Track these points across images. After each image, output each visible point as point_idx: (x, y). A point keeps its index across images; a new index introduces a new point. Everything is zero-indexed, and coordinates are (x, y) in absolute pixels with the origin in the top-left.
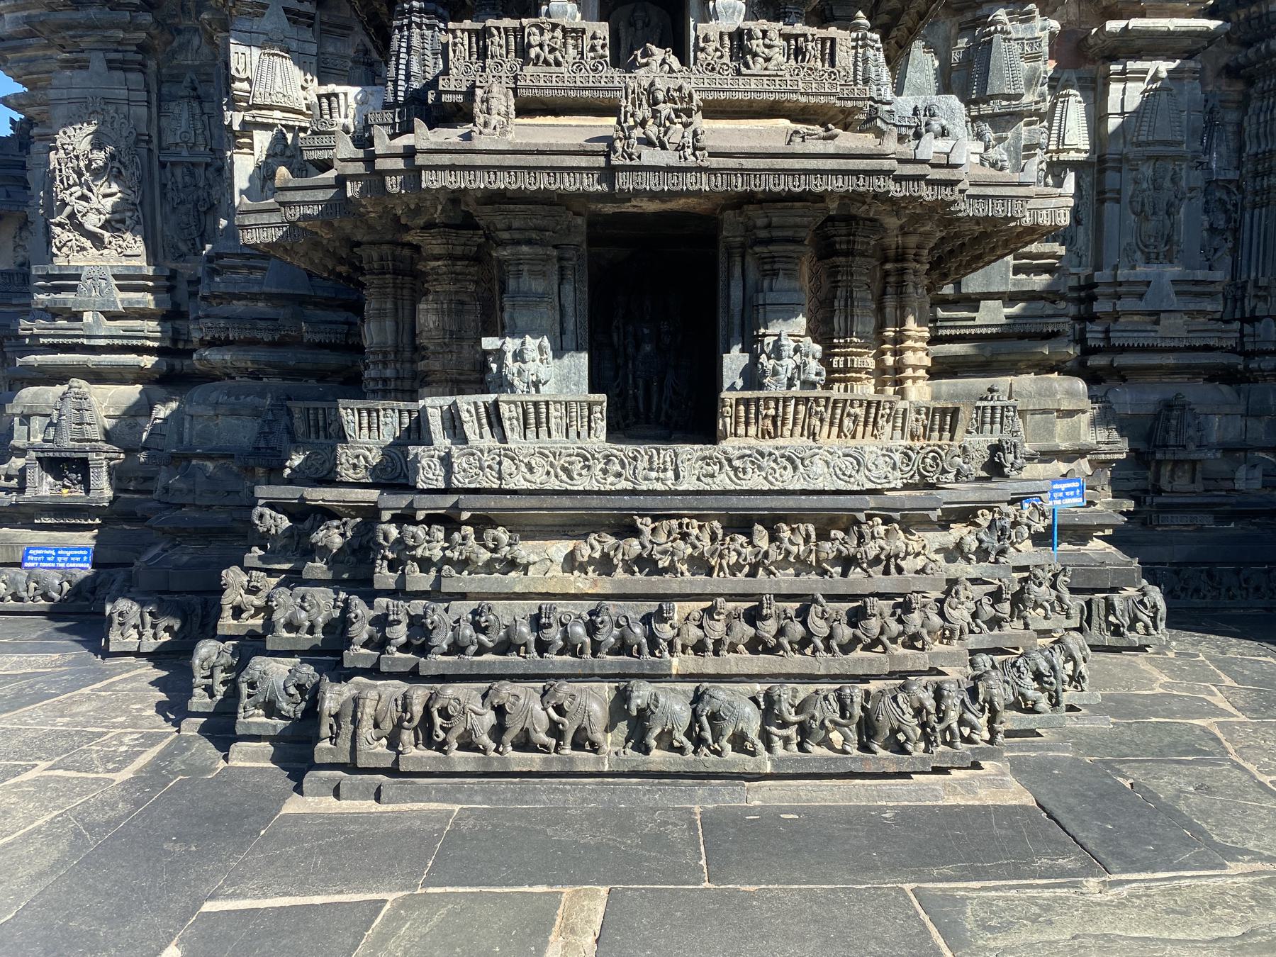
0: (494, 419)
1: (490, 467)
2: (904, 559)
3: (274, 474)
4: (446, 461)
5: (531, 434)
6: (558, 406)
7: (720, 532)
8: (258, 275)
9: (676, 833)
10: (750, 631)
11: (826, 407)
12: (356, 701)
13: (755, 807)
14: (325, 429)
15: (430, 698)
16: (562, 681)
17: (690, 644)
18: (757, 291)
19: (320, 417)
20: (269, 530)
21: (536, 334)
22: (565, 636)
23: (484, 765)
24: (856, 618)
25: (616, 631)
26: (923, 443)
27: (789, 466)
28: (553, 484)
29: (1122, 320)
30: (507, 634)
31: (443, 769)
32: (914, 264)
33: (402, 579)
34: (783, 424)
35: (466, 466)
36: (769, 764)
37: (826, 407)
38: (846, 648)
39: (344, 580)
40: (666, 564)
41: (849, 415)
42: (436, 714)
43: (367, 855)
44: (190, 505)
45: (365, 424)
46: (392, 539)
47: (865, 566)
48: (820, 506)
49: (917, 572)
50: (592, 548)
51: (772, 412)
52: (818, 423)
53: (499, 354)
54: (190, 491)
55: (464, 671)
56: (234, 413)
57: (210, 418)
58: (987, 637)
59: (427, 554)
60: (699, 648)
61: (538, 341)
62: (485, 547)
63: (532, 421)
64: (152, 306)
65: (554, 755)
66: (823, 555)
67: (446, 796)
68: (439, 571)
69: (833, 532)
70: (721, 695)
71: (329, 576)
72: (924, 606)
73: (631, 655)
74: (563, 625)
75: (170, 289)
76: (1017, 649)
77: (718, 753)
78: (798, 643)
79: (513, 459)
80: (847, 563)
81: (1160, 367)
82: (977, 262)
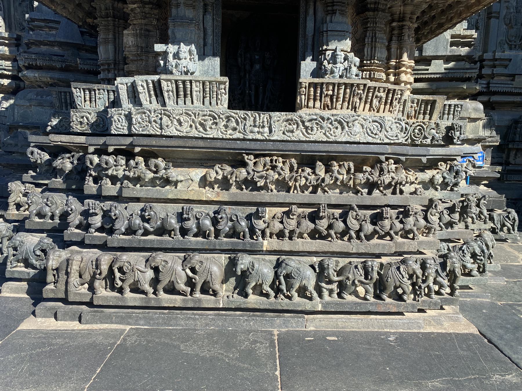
0: (158, 92)
1: (155, 121)
2: (404, 185)
3: (40, 129)
4: (129, 117)
5: (181, 102)
6: (198, 84)
7: (296, 166)
8: (54, 32)
9: (262, 350)
10: (312, 226)
11: (363, 90)
12: (68, 260)
13: (311, 331)
14: (71, 104)
15: (113, 261)
16: (196, 253)
17: (275, 232)
18: (323, 24)
19: (68, 97)
20: (36, 161)
21: (188, 43)
22: (198, 226)
23: (146, 302)
24: (376, 219)
25: (230, 224)
26: (414, 120)
27: (339, 127)
28: (194, 133)
29: (495, 78)
30: (162, 223)
31: (120, 304)
32: (409, 23)
33: (100, 189)
34: (337, 101)
35: (140, 120)
36: (320, 305)
37: (363, 90)
38: (369, 238)
39: (73, 190)
40: (262, 184)
41: (377, 97)
42: (116, 271)
43: (59, 363)
44: (18, 152)
45: (88, 98)
46: (95, 164)
47: (381, 188)
48: (358, 150)
49: (411, 194)
50: (217, 173)
51: (330, 93)
52: (358, 101)
53: (165, 54)
54: (16, 145)
55: (135, 245)
56: (40, 105)
57: (27, 106)
58: (446, 233)
59: (115, 173)
60: (280, 235)
61: (189, 47)
62: (150, 170)
63: (182, 93)
64: (8, 53)
65: (189, 297)
66: (358, 181)
67: (122, 320)
68: (121, 184)
69: (365, 167)
70: (292, 264)
71: (64, 186)
72: (416, 214)
73: (239, 238)
74: (197, 219)
75: (18, 45)
76: (459, 240)
77: (290, 298)
78: (340, 234)
79: (169, 117)
80: (371, 186)
81: (513, 103)
82: (441, 28)
